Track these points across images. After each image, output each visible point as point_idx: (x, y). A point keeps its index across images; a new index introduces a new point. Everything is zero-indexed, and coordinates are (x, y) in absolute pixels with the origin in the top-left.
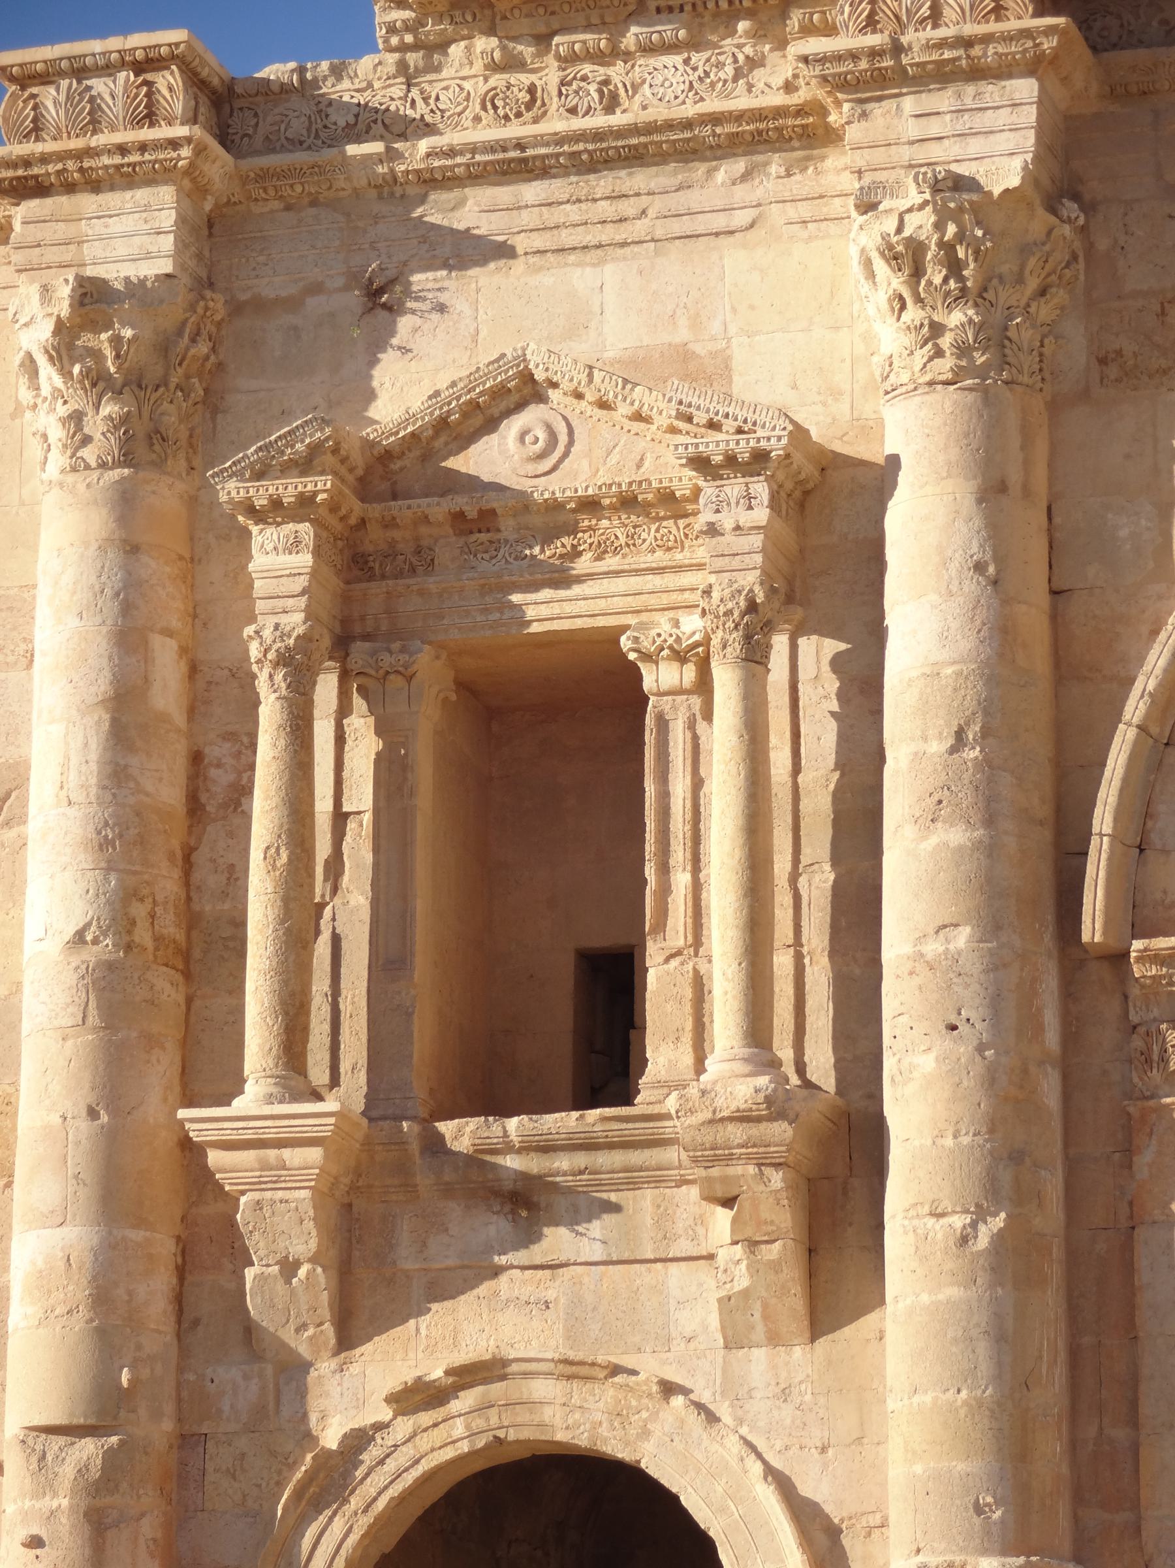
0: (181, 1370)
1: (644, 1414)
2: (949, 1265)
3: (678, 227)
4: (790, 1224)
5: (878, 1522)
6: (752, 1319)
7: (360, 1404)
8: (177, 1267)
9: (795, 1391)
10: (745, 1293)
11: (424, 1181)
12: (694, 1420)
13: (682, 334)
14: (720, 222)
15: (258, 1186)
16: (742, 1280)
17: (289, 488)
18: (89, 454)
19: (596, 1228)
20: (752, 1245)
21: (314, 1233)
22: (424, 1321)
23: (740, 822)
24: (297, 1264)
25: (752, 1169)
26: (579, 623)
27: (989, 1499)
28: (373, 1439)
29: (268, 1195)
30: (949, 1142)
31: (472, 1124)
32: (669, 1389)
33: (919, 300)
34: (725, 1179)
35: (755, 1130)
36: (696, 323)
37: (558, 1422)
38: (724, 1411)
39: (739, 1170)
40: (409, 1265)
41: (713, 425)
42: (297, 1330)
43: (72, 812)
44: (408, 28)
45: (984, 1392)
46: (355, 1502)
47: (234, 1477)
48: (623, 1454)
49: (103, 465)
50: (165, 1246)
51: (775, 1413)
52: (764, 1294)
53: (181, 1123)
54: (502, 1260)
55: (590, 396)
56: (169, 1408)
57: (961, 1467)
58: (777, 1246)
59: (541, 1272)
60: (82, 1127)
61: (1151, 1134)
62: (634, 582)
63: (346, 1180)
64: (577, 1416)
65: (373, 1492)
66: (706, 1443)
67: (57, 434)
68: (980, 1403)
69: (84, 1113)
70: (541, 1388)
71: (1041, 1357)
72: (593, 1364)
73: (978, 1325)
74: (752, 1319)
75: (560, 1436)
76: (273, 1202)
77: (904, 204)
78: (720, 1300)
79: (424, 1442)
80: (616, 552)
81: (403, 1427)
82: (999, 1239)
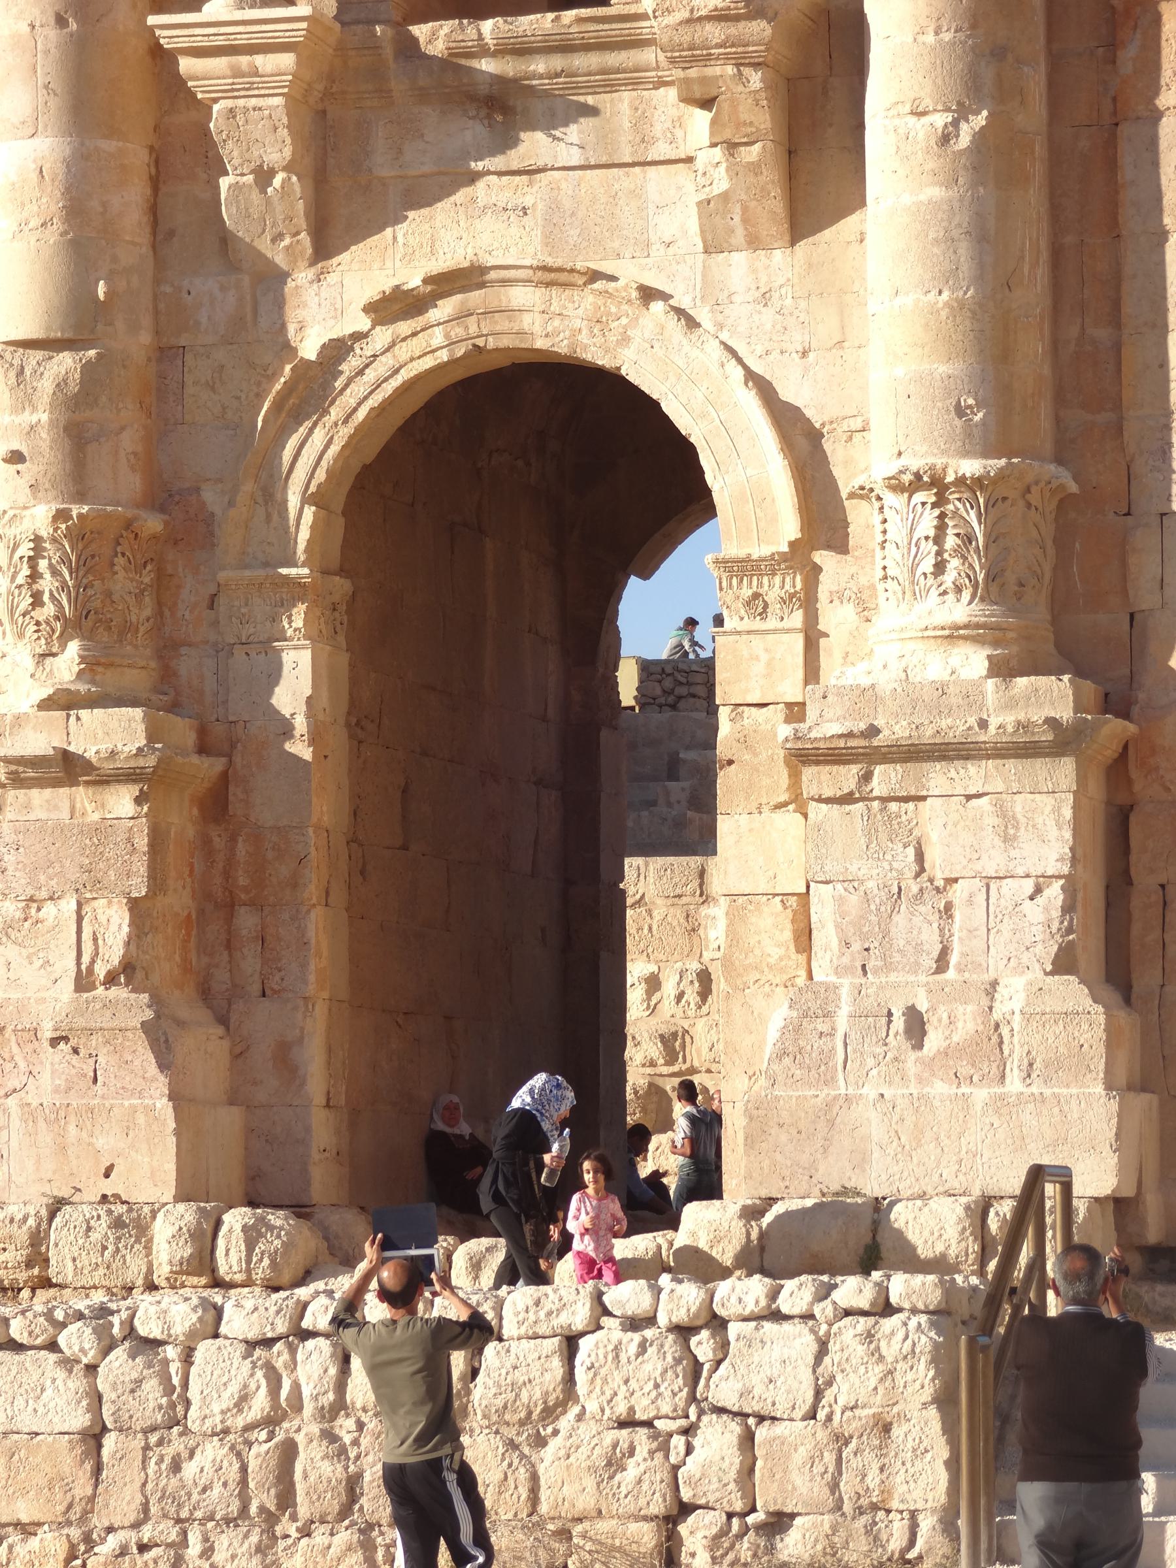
0: (157, 281)
1: (624, 321)
2: (931, 165)
4: (769, 125)
5: (859, 426)
6: (732, 223)
7: (339, 313)
8: (151, 178)
9: (776, 295)
10: (725, 197)
11: (398, 85)
12: (674, 326)
15: (230, 93)
16: (721, 183)
19: (573, 132)
20: (731, 147)
21: (288, 141)
22: (401, 229)
24: (272, 173)
25: (730, 70)
27: (971, 401)
28: (352, 349)
29: (241, 102)
30: (930, 38)
31: (446, 27)
32: (648, 294)
34: (703, 80)
35: (733, 30)
37: (537, 329)
38: (703, 315)
39: (718, 70)
40: (385, 172)
42: (274, 240)
45: (965, 293)
46: (335, 413)
48: (603, 361)
50: (138, 157)
51: (756, 317)
52: (744, 197)
53: (151, 29)
54: (478, 166)
56: (147, 321)
57: (943, 369)
58: (757, 147)
59: (518, 178)
60: (50, 35)
61: (1135, 27)
63: (320, 87)
64: (557, 322)
65: (353, 402)
66: (687, 348)
68: (961, 304)
69: (52, 21)
70: (520, 296)
71: (1022, 258)
72: (572, 271)
73: (959, 225)
74: (732, 223)
75: (540, 344)
76: (246, 110)
78: (699, 204)
79: (403, 352)
81: (382, 336)
82: (980, 137)
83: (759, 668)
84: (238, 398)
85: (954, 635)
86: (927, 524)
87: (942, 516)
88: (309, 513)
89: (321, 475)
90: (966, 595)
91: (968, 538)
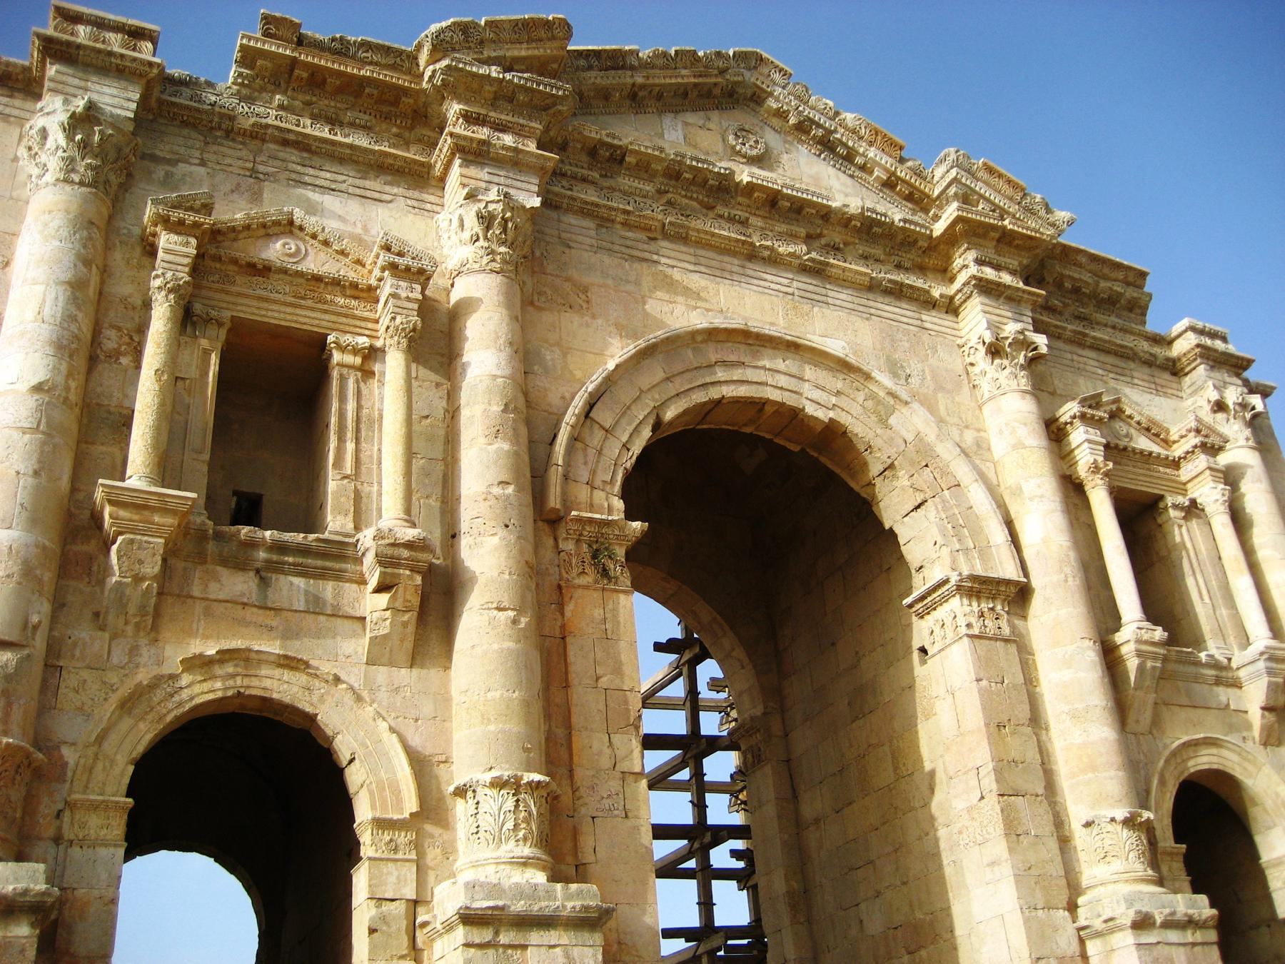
1: (322, 691)
2: (508, 632)
3: (358, 191)
5: (444, 759)
10: (385, 637)
12: (349, 699)
13: (359, 230)
14: (377, 195)
17: (191, 218)
18: (76, 178)
23: (405, 417)
24: (143, 579)
26: (305, 327)
29: (139, 537)
30: (507, 577)
32: (337, 680)
33: (486, 238)
34: (393, 575)
36: (365, 228)
38: (365, 694)
39: (401, 571)
41: (400, 254)
43: (46, 326)
44: (247, 77)
47: (77, 692)
48: (309, 709)
49: (81, 183)
55: (320, 238)
60: (30, 481)
62: (333, 318)
66: (355, 709)
67: (54, 164)
69: (31, 472)
75: (275, 696)
76: (140, 542)
77: (488, 199)
79: (197, 689)
80: (325, 303)
81: (186, 679)
83: (392, 879)
84: (93, 699)
85: (525, 863)
86: (510, 804)
87: (518, 801)
88: (131, 769)
89: (141, 749)
90: (528, 844)
91: (530, 814)
